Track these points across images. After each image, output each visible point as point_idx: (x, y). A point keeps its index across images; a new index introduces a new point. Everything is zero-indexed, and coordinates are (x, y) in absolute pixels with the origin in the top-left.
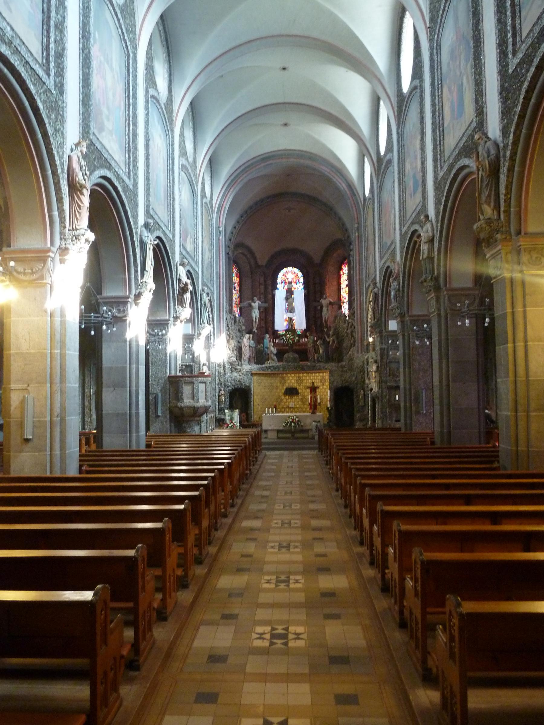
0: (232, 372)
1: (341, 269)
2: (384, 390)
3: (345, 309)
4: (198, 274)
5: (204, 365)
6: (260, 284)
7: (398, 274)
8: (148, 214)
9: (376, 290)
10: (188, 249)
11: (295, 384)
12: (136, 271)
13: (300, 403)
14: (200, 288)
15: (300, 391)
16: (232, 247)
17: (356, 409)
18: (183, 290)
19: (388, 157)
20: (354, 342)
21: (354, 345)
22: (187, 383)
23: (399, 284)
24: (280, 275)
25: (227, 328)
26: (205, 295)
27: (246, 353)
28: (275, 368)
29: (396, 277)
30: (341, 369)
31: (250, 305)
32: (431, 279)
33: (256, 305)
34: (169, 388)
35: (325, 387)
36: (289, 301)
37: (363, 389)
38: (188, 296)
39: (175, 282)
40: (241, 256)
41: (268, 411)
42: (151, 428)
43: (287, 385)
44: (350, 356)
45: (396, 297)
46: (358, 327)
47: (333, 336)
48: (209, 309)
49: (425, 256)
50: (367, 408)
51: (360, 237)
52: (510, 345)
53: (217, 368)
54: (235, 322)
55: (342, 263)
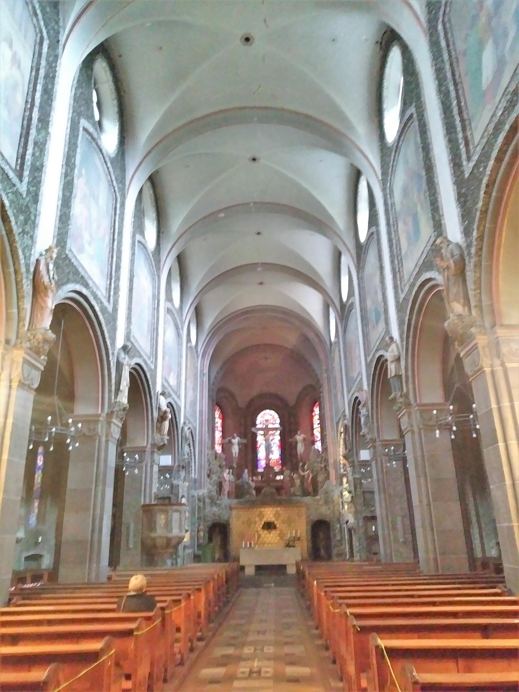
1: (312, 411)
5: (183, 496)
9: (346, 422)
10: (171, 384)
12: (110, 391)
13: (278, 538)
15: (278, 526)
17: (333, 544)
18: (162, 418)
20: (328, 475)
23: (368, 411)
25: (208, 464)
26: (186, 428)
27: (226, 488)
32: (401, 396)
33: (236, 441)
36: (267, 437)
38: (167, 424)
39: (154, 411)
41: (246, 545)
45: (366, 424)
47: (307, 470)
49: (393, 375)
50: (344, 542)
51: (328, 378)
54: (216, 458)
55: (314, 405)
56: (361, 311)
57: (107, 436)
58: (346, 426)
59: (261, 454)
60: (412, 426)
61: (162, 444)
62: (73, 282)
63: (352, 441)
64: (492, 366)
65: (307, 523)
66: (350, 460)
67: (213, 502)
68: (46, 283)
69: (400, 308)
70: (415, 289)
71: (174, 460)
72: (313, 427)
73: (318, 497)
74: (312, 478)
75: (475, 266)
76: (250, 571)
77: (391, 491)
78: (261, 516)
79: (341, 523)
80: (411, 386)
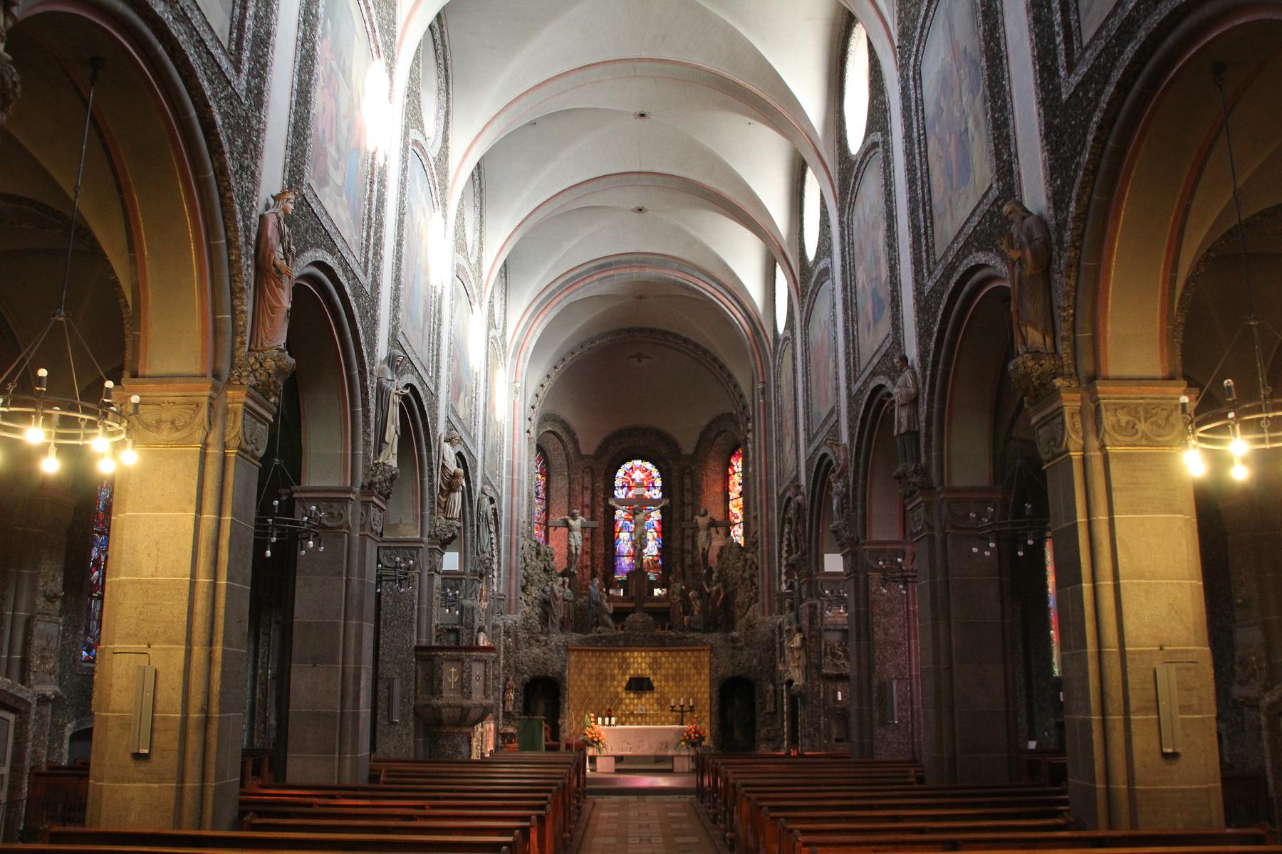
1: (730, 465)
4: (476, 461)
5: (481, 629)
6: (584, 488)
7: (846, 466)
8: (394, 341)
9: (799, 498)
11: (648, 671)
12: (367, 443)
13: (656, 706)
14: (479, 488)
15: (655, 684)
16: (535, 419)
18: (450, 487)
20: (756, 594)
21: (757, 601)
22: (452, 660)
23: (847, 486)
24: (620, 473)
25: (524, 565)
27: (559, 612)
29: (842, 473)
30: (732, 645)
31: (567, 525)
32: (916, 471)
34: (417, 671)
35: (703, 677)
37: (773, 682)
38: (457, 496)
39: (435, 472)
43: (632, 672)
44: (748, 621)
45: (842, 508)
47: (717, 582)
49: (903, 430)
51: (767, 406)
52: (1086, 586)
54: (538, 554)
55: (732, 453)
56: (845, 289)
57: (363, 527)
58: (799, 505)
59: (624, 542)
60: (931, 528)
61: (450, 535)
62: (312, 246)
63: (810, 537)
64: (1084, 449)
65: (711, 681)
67: (532, 638)
68: (278, 262)
69: (923, 307)
70: (956, 277)
71: (463, 560)
72: (729, 496)
73: (736, 634)
74: (726, 597)
75: (1069, 266)
78: (624, 665)
79: (778, 682)
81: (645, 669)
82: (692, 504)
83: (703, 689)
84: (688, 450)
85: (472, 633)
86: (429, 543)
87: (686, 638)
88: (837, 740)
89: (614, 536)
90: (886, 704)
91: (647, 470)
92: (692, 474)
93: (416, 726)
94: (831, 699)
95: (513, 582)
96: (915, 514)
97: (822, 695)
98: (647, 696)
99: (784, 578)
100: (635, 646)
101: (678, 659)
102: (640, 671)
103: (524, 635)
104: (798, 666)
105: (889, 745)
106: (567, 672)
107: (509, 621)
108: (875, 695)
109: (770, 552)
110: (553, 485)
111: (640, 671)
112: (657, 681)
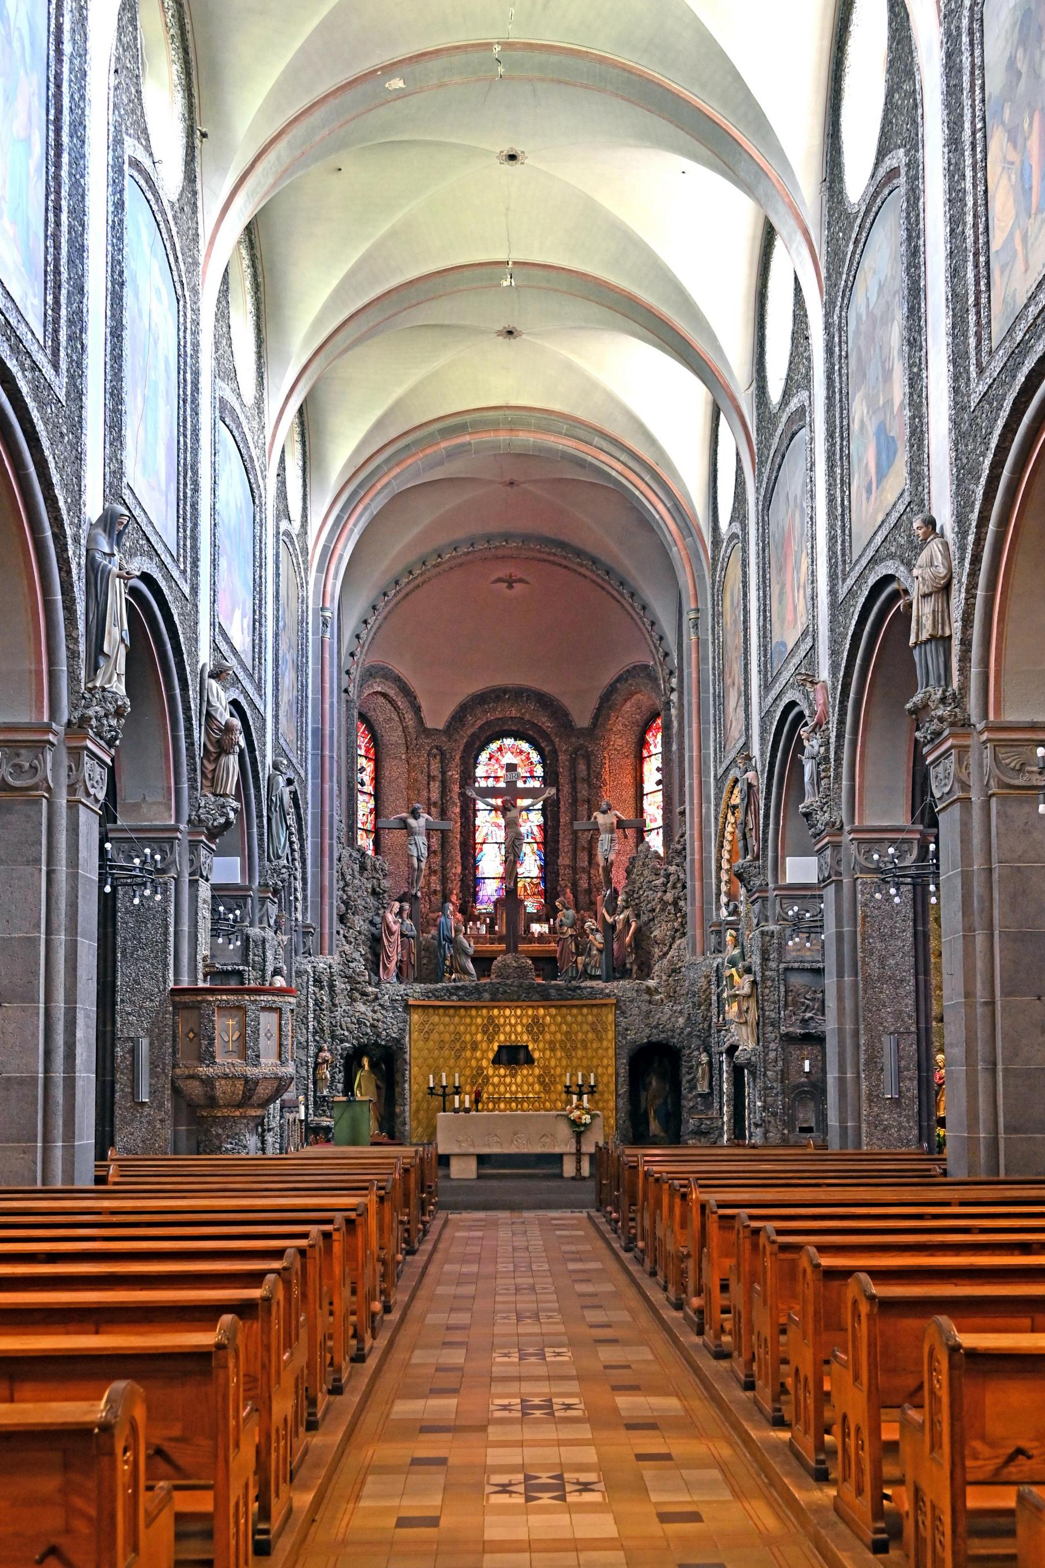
0: (354, 1000)
1: (642, 743)
2: (773, 1046)
3: (655, 842)
4: (264, 720)
5: (277, 972)
6: (430, 778)
7: (826, 713)
9: (750, 775)
11: (525, 1037)
13: (537, 1087)
14: (269, 761)
15: (536, 1055)
17: (687, 1104)
19: (794, 404)
20: (683, 925)
22: (226, 1009)
24: (484, 757)
25: (342, 884)
26: (281, 780)
28: (471, 993)
29: (819, 724)
30: (646, 997)
31: (404, 825)
32: (943, 700)
34: (175, 1024)
35: (605, 1043)
36: (509, 814)
37: (707, 1050)
40: (381, 700)
42: (117, 1139)
43: (502, 1037)
44: (671, 962)
46: (694, 885)
47: (627, 908)
48: (291, 820)
50: (716, 1100)
53: (311, 989)
54: (363, 868)
55: (646, 728)
57: (72, 789)
58: (750, 786)
60: (965, 787)
61: (222, 820)
63: (766, 833)
66: (756, 882)
67: (356, 992)
71: (248, 869)
72: (642, 788)
73: (651, 983)
74: (638, 930)
76: (463, 1170)
77: (875, 971)
78: (491, 1028)
79: (714, 1050)
80: (974, 671)
81: (522, 1033)
82: (589, 801)
83: (605, 1062)
84: (582, 720)
85: (263, 977)
86: (190, 833)
87: (579, 988)
88: (803, 1130)
89: (475, 849)
90: (882, 1070)
91: (521, 752)
92: (588, 757)
93: (176, 1108)
94: (793, 1071)
95: (327, 909)
96: (940, 769)
97: (780, 1063)
98: (525, 1072)
99: (724, 899)
100: (507, 1001)
101: (569, 1018)
102: (513, 1037)
103: (343, 986)
104: (746, 1023)
105: (884, 1130)
106: (407, 1039)
107: (321, 965)
108: (863, 1057)
109: (703, 863)
110: (386, 773)
111: (513, 1037)
112: (540, 1051)
